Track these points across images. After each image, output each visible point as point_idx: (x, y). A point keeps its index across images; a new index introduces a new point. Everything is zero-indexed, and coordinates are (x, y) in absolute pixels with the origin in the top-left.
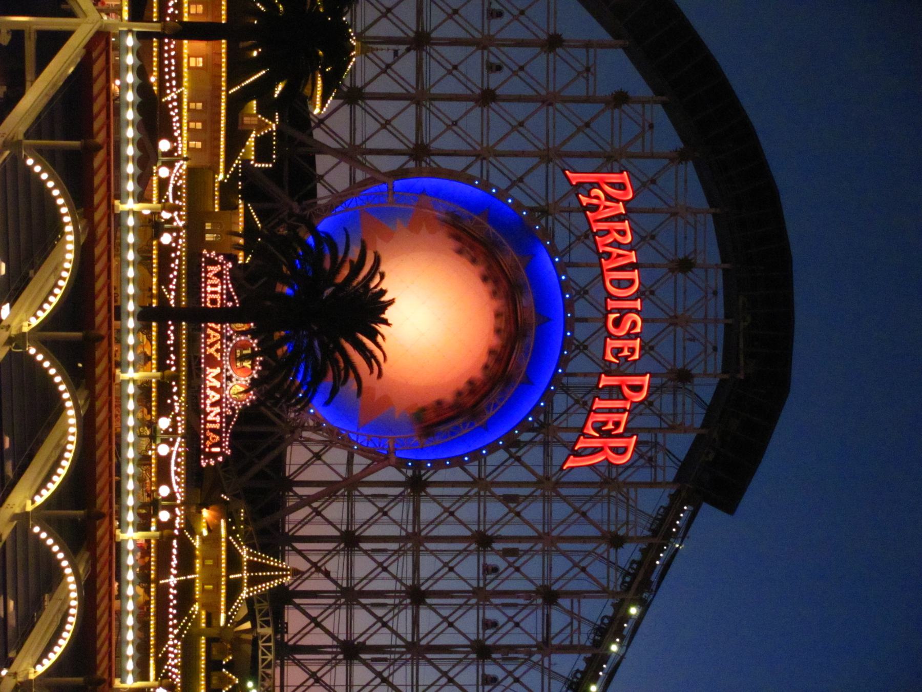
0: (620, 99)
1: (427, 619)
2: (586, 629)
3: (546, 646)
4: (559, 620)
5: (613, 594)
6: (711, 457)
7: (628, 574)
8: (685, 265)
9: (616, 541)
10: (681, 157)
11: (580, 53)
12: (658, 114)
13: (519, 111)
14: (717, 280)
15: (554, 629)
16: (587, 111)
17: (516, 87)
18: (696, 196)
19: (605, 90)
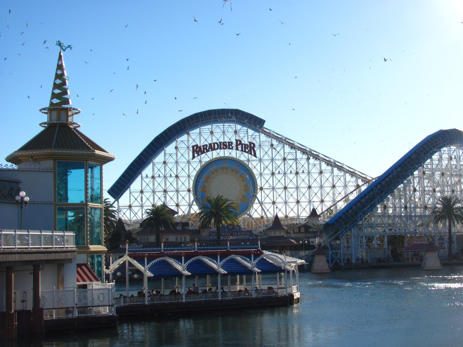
0: (176, 148)
1: (291, 185)
2: (292, 151)
3: (296, 159)
4: (290, 157)
5: (284, 145)
6: (253, 125)
7: (279, 142)
8: (212, 133)
9: (272, 145)
10: (188, 134)
11: (167, 157)
12: (180, 139)
13: (180, 169)
14: (215, 125)
15: (292, 158)
16: (179, 155)
17: (175, 171)
18: (197, 130)
19: (174, 151)
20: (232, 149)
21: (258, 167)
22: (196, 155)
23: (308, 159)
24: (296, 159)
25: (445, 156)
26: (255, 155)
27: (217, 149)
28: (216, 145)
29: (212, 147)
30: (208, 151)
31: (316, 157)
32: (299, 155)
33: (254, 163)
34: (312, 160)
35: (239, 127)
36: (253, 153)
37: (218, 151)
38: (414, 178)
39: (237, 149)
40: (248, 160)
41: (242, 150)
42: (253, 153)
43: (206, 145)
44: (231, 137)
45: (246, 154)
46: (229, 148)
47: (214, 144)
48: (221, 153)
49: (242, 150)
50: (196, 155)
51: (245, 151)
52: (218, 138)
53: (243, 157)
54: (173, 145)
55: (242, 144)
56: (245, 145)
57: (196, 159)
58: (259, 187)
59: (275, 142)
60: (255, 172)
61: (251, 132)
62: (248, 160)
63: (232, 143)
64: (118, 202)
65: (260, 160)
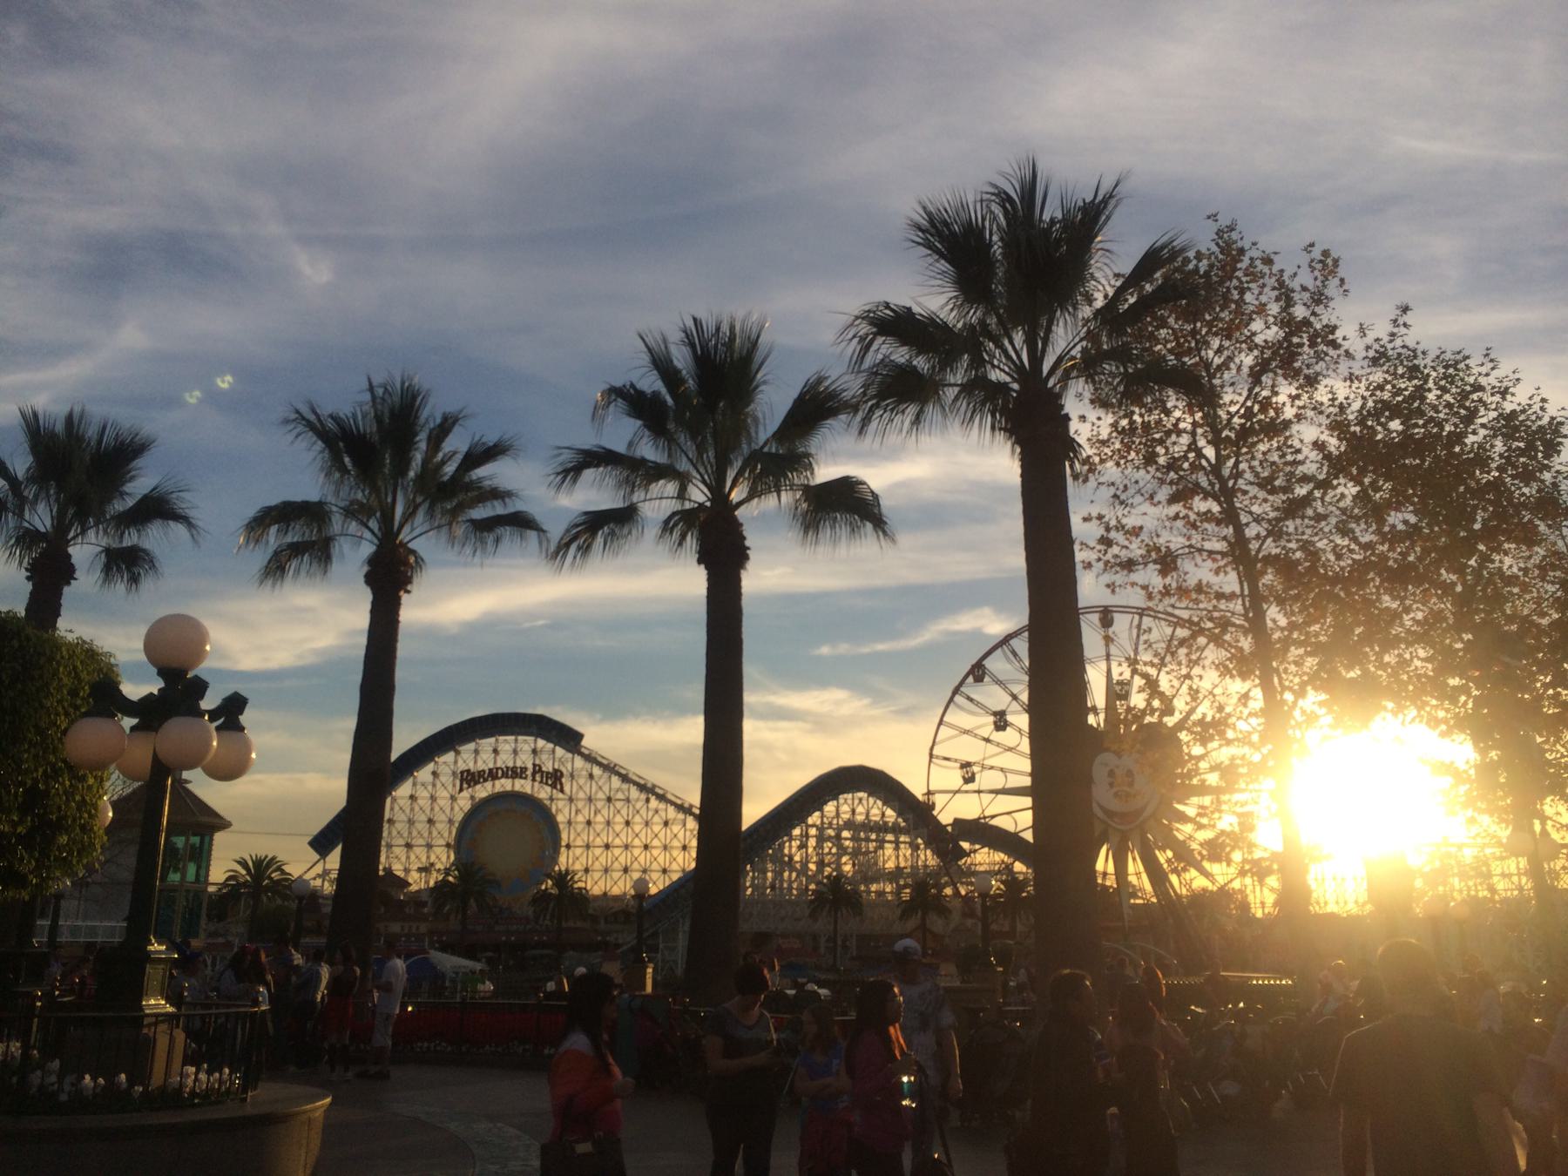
0: (435, 774)
9: (591, 776)
10: (458, 753)
11: (418, 787)
16: (439, 785)
18: (471, 746)
19: (430, 778)
20: (525, 778)
21: (566, 811)
22: (465, 786)
23: (648, 800)
24: (628, 800)
25: (845, 808)
26: (562, 791)
27: (502, 777)
28: (500, 772)
29: (493, 775)
30: (485, 780)
31: (662, 798)
32: (634, 793)
33: (561, 804)
34: (654, 803)
35: (541, 743)
36: (559, 787)
37: (503, 781)
38: (791, 840)
39: (534, 780)
40: (551, 799)
41: (541, 782)
42: (559, 787)
43: (484, 771)
44: (526, 760)
45: (548, 789)
46: (521, 778)
47: (497, 769)
48: (504, 785)
49: (541, 782)
50: (465, 786)
51: (547, 784)
52: (505, 760)
53: (543, 793)
54: (430, 767)
55: (543, 772)
56: (548, 773)
57: (465, 794)
58: (563, 843)
59: (597, 771)
60: (560, 818)
61: (560, 751)
62: (551, 799)
63: (526, 769)
64: (325, 862)
65: (571, 800)
